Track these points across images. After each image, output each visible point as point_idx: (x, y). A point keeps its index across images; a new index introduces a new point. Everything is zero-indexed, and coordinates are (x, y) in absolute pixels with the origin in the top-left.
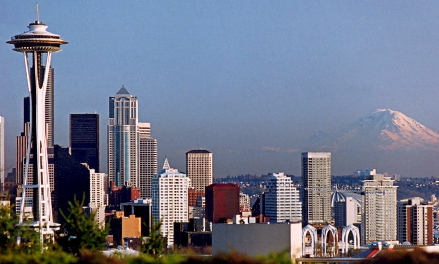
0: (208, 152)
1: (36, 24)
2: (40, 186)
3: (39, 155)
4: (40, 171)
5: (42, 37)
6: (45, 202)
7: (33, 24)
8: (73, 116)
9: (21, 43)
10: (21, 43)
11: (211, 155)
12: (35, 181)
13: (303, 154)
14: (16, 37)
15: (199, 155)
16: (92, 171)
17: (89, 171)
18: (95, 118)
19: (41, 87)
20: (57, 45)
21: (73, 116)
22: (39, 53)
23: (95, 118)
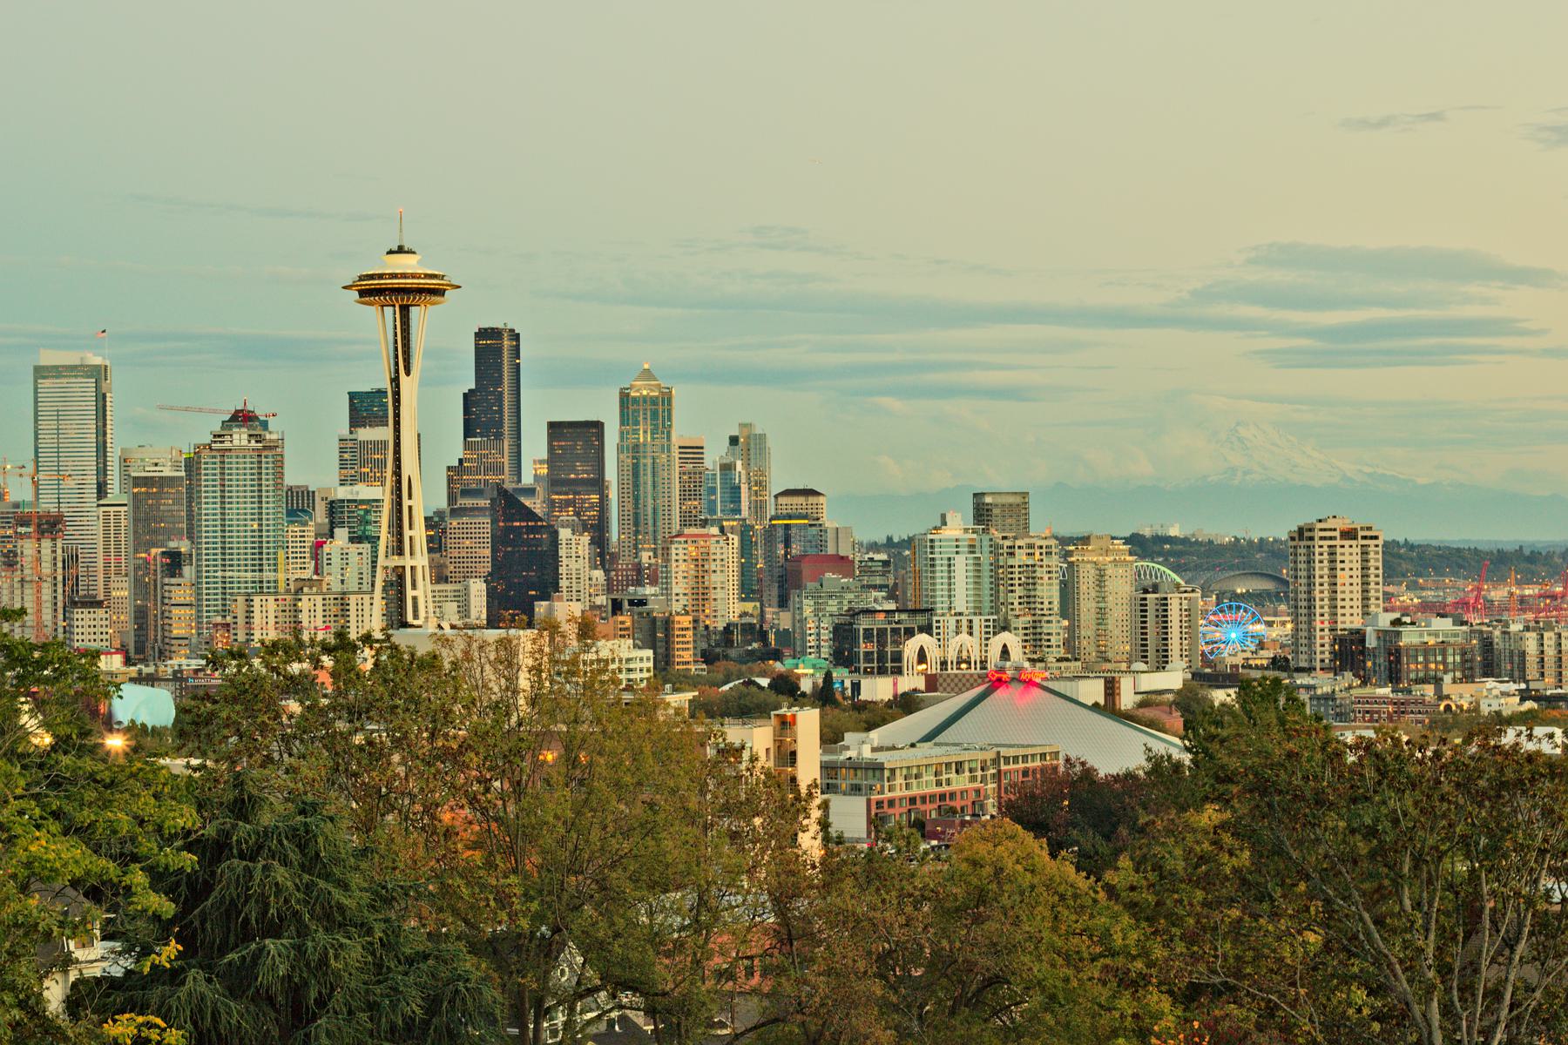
0: (818, 494)
1: (401, 250)
2: (407, 562)
3: (406, 503)
4: (407, 533)
5: (414, 276)
6: (419, 593)
7: (391, 252)
8: (553, 426)
9: (372, 291)
10: (372, 291)
11: (821, 499)
12: (400, 552)
13: (975, 495)
14: (361, 278)
15: (801, 500)
16: (564, 534)
17: (556, 533)
18: (598, 426)
19: (408, 374)
20: (438, 292)
21: (553, 426)
22: (405, 310)
23: (598, 426)
